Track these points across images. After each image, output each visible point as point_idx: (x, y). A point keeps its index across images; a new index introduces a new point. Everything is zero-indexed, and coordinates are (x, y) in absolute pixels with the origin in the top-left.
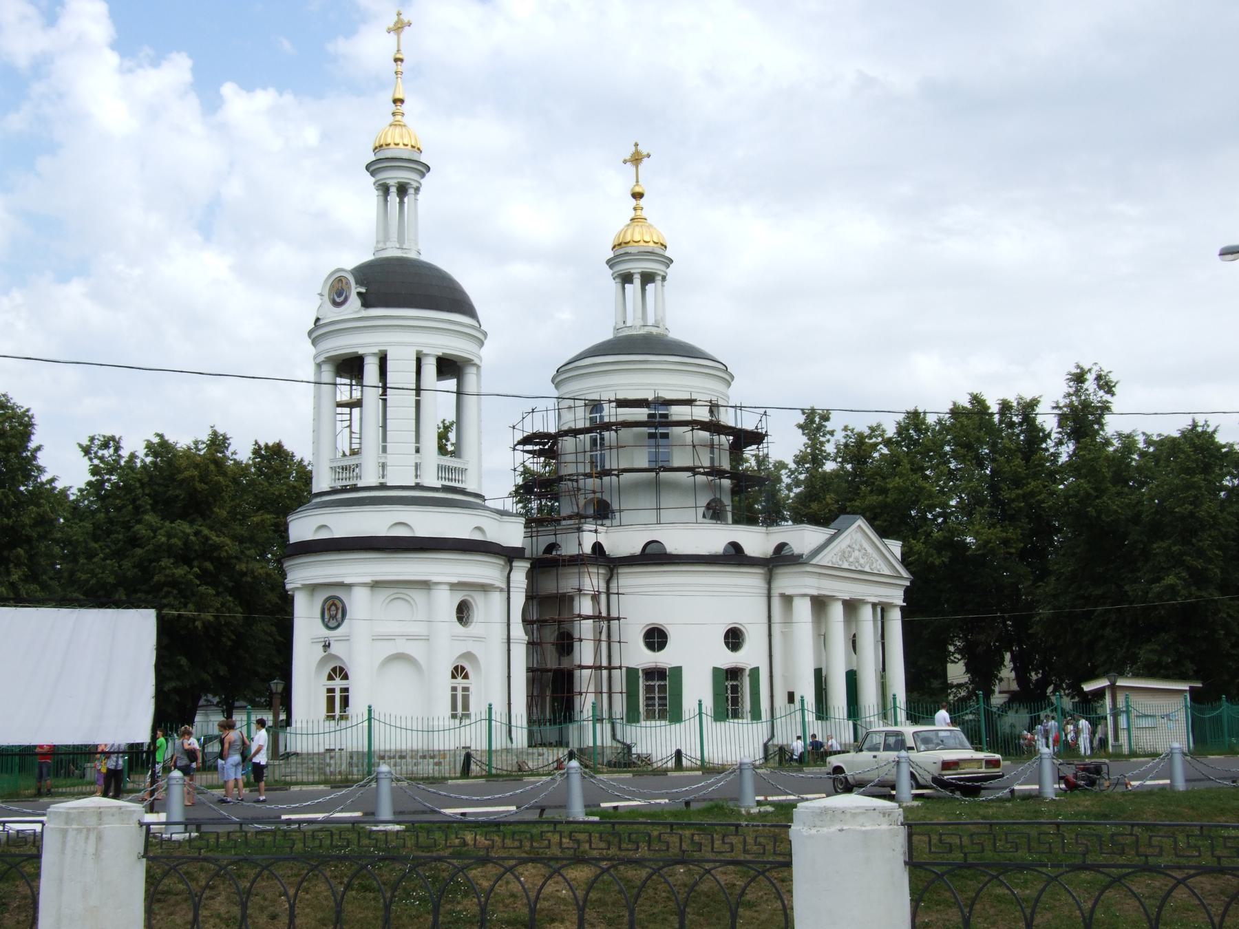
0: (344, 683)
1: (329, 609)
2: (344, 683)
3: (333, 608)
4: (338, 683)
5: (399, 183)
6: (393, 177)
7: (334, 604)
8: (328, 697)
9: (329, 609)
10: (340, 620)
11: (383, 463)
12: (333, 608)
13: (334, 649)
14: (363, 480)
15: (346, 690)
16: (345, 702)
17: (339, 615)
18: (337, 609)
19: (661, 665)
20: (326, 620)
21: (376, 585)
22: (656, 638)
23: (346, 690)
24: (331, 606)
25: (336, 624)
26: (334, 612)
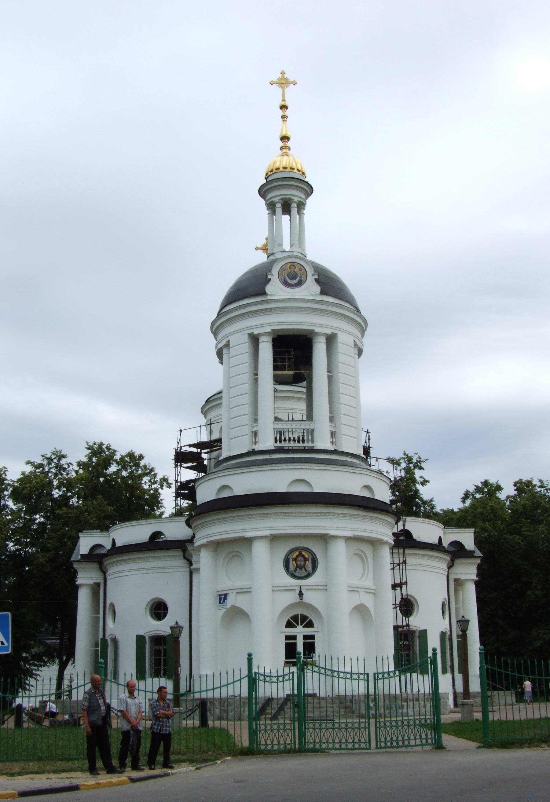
0: (309, 631)
2: (309, 631)
4: (300, 631)
5: (282, 199)
6: (276, 195)
7: (300, 555)
8: (286, 644)
11: (255, 432)
12: (300, 558)
14: (260, 445)
15: (312, 637)
16: (310, 648)
17: (309, 565)
23: (312, 637)
24: (297, 556)
25: (305, 574)
26: (302, 563)
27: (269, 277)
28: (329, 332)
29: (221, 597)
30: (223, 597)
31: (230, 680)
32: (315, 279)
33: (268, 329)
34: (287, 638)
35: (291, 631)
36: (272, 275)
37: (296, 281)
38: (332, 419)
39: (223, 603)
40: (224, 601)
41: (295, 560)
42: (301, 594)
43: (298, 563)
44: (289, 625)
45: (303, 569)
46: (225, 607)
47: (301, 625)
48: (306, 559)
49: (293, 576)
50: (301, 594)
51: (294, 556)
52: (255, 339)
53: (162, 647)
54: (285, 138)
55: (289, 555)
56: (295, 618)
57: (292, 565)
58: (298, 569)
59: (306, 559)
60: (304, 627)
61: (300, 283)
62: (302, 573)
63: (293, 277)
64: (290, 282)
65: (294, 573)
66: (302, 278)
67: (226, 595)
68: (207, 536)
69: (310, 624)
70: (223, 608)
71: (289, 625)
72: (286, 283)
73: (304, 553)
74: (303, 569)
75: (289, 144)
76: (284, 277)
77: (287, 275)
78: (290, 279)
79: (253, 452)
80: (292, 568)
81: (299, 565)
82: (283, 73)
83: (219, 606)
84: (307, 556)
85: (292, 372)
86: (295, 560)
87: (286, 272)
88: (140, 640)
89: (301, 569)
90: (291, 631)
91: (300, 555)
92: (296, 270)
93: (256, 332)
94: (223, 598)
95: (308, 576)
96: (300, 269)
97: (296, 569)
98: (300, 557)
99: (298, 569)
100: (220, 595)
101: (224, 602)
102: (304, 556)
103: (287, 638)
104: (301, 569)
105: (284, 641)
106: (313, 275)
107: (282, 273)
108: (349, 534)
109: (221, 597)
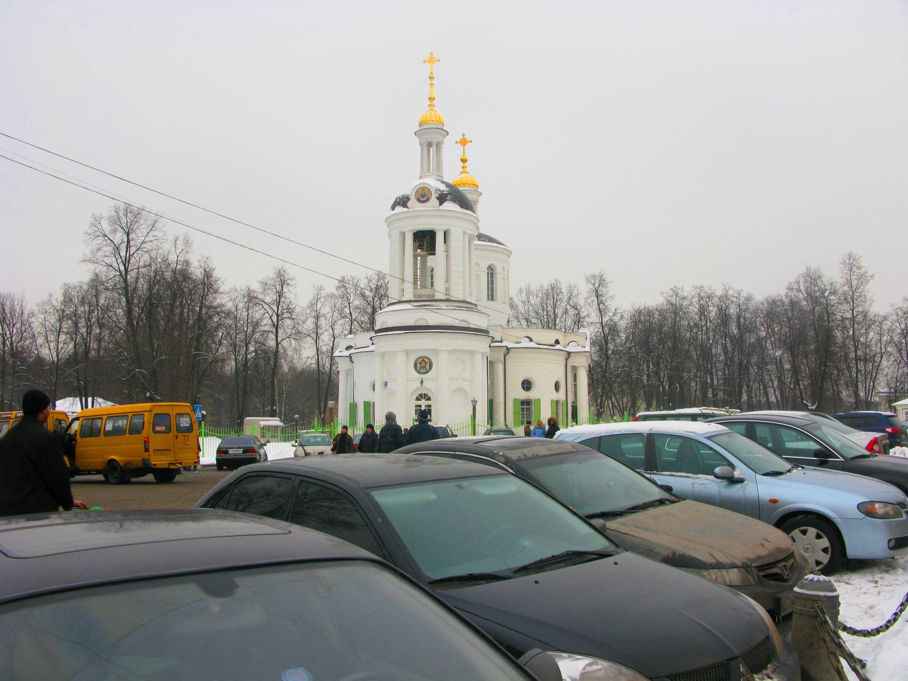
0: (428, 403)
2: (428, 403)
7: (423, 360)
8: (416, 409)
12: (423, 362)
13: (426, 383)
17: (428, 366)
19: (530, 398)
21: (451, 352)
22: (527, 385)
23: (430, 406)
24: (421, 362)
26: (424, 365)
28: (445, 228)
31: (459, 428)
32: (437, 198)
34: (416, 406)
35: (419, 403)
37: (425, 199)
38: (447, 281)
41: (420, 363)
42: (422, 382)
43: (422, 365)
44: (418, 399)
48: (426, 363)
49: (419, 372)
50: (422, 382)
51: (420, 361)
52: (403, 235)
54: (431, 99)
56: (421, 395)
57: (419, 366)
59: (426, 363)
60: (427, 400)
62: (424, 371)
63: (423, 197)
64: (422, 199)
67: (387, 382)
69: (429, 399)
71: (418, 399)
72: (419, 201)
73: (425, 359)
75: (434, 102)
80: (418, 368)
82: (431, 54)
84: (426, 361)
86: (420, 363)
87: (420, 193)
89: (423, 368)
90: (419, 403)
91: (423, 360)
92: (426, 191)
93: (403, 230)
94: (386, 384)
95: (427, 372)
96: (428, 191)
97: (420, 368)
103: (416, 406)
104: (423, 368)
105: (415, 408)
108: (450, 348)
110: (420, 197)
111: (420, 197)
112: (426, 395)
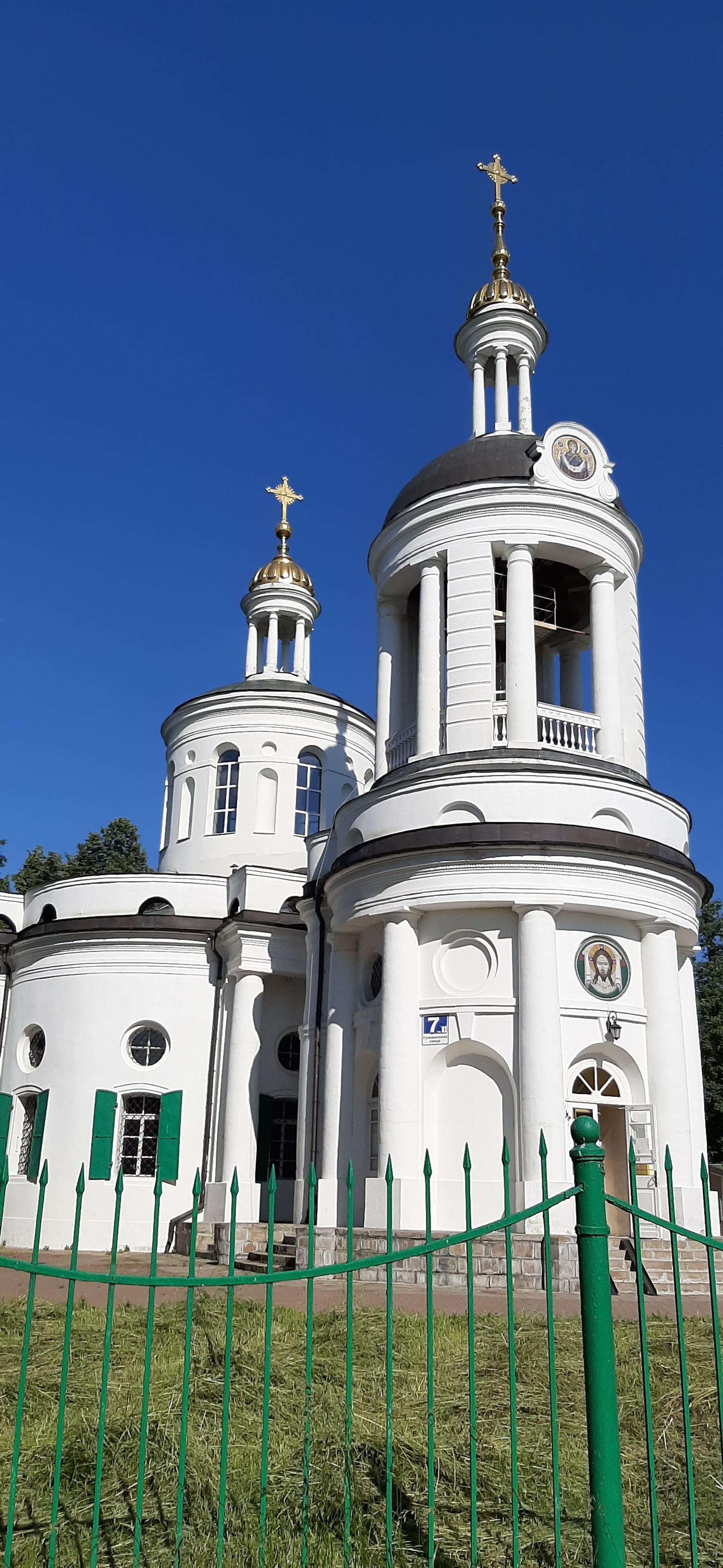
1: (594, 960)
3: (602, 958)
9: (594, 960)
10: (618, 981)
12: (602, 958)
18: (611, 963)
20: (588, 978)
24: (597, 954)
25: (610, 990)
26: (606, 967)
27: (539, 450)
29: (430, 1019)
30: (437, 1019)
33: (534, 540)
36: (543, 448)
37: (578, 469)
39: (436, 1032)
40: (438, 1029)
43: (599, 966)
45: (607, 979)
46: (443, 1041)
47: (599, 1089)
49: (592, 990)
50: (613, 1028)
53: (143, 1117)
55: (583, 949)
58: (599, 977)
60: (603, 1094)
61: (584, 475)
62: (604, 987)
63: (576, 462)
64: (570, 468)
65: (593, 985)
66: (588, 467)
68: (412, 896)
69: (613, 1091)
70: (435, 1043)
71: (579, 1088)
72: (563, 468)
74: (607, 979)
76: (561, 457)
77: (566, 455)
78: (570, 464)
79: (502, 751)
81: (600, 970)
83: (423, 1038)
85: (554, 627)
88: (104, 1099)
89: (604, 980)
93: (509, 540)
95: (616, 994)
97: (596, 978)
98: (602, 956)
99: (599, 977)
100: (426, 1017)
101: (441, 1029)
102: (608, 956)
104: (604, 980)
106: (606, 467)
107: (558, 450)
109: (430, 1019)
110: (565, 460)
111: (565, 460)
112: (604, 1076)
